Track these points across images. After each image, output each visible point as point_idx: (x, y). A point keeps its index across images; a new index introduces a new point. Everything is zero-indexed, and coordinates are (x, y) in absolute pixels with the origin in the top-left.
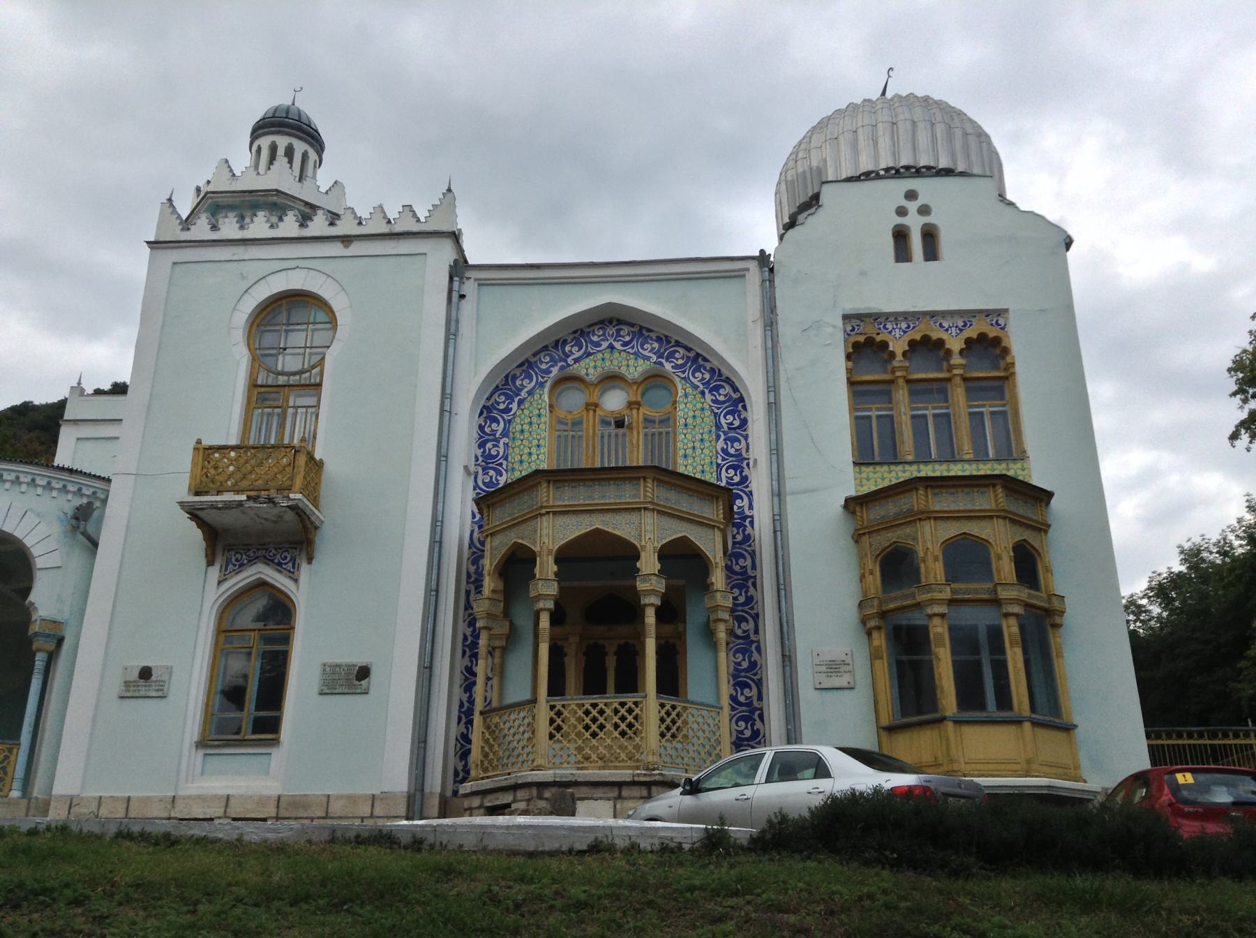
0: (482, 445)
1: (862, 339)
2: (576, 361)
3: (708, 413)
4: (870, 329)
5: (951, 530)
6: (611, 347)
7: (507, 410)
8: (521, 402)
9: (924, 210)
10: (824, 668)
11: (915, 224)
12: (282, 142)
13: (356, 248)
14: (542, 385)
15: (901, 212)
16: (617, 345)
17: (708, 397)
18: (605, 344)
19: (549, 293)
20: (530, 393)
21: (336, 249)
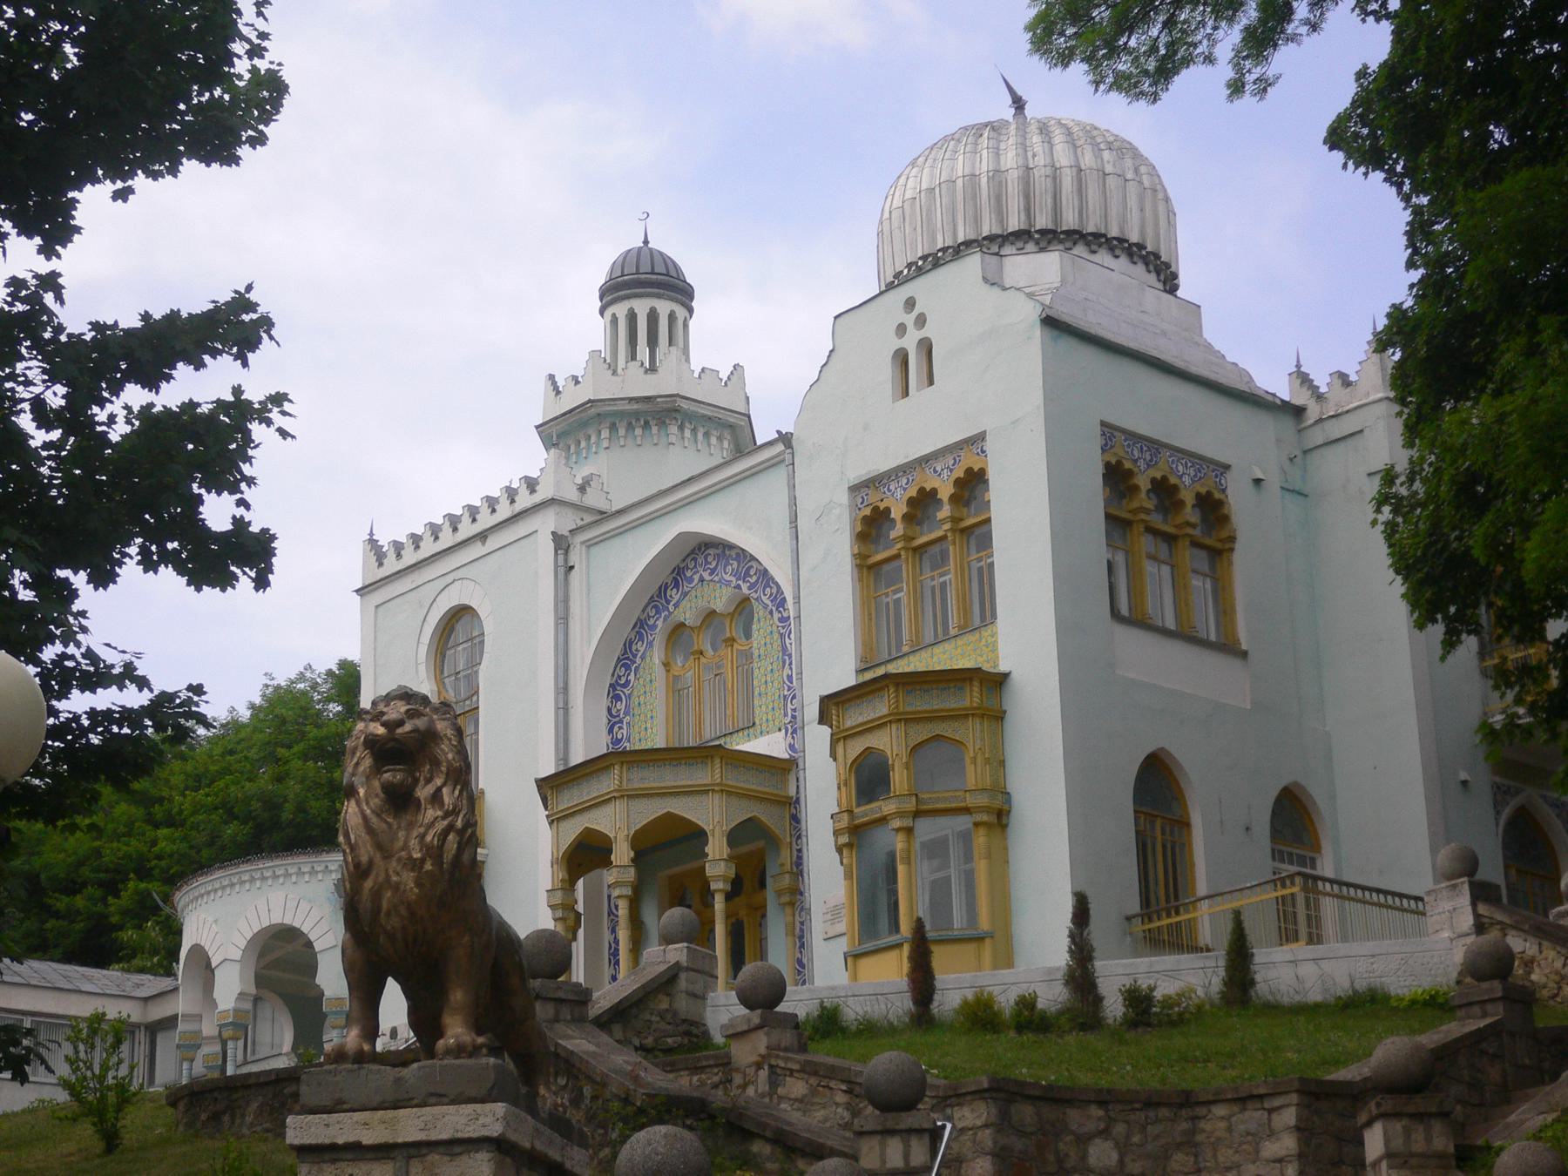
0: (611, 731)
1: (868, 511)
2: (676, 606)
3: (776, 636)
4: (873, 497)
5: (922, 732)
6: (702, 580)
7: (628, 682)
8: (637, 669)
9: (921, 321)
10: (829, 916)
11: (910, 342)
12: (642, 307)
13: (494, 542)
14: (650, 644)
15: (901, 330)
16: (706, 576)
17: (776, 615)
18: (696, 577)
19: (656, 525)
20: (643, 658)
21: (477, 550)
